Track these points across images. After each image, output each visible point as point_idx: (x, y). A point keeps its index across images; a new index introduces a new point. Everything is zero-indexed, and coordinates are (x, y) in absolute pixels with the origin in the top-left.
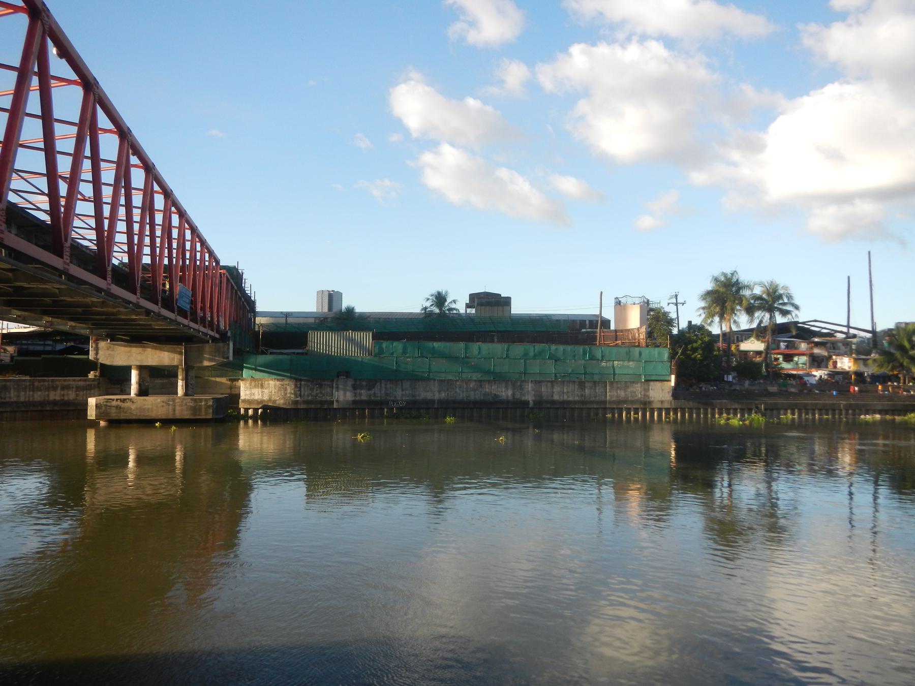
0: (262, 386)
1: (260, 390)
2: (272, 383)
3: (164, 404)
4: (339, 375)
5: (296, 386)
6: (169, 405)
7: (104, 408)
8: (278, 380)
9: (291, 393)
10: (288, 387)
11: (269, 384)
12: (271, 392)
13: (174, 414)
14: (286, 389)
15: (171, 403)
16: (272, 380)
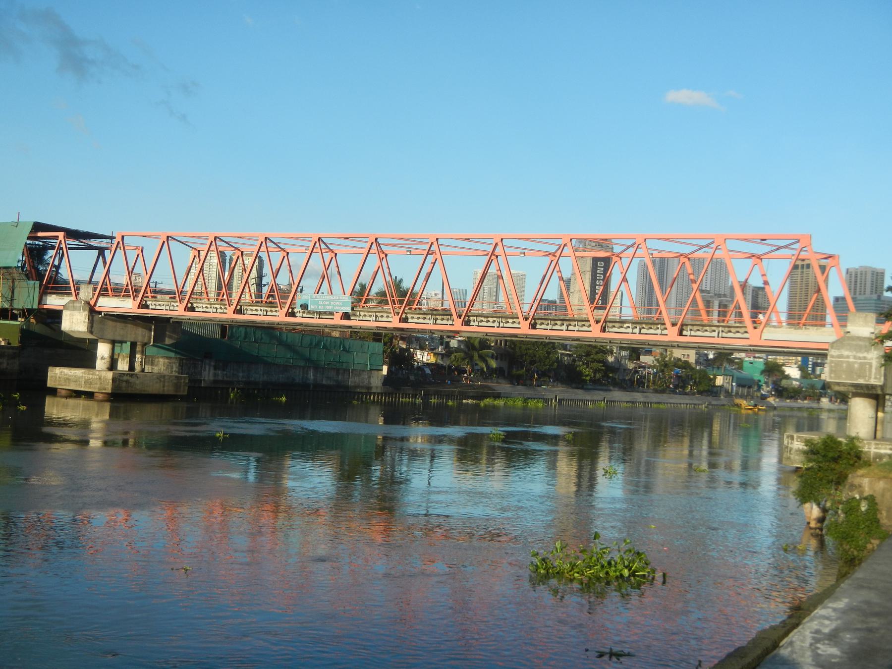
0: (152, 364)
1: (150, 367)
2: (161, 360)
3: (158, 381)
4: (208, 355)
5: (180, 365)
6: (160, 380)
7: (118, 382)
8: (167, 358)
9: (175, 371)
10: (174, 366)
11: (158, 361)
12: (160, 370)
13: (164, 390)
14: (172, 368)
15: (162, 379)
16: (162, 357)
